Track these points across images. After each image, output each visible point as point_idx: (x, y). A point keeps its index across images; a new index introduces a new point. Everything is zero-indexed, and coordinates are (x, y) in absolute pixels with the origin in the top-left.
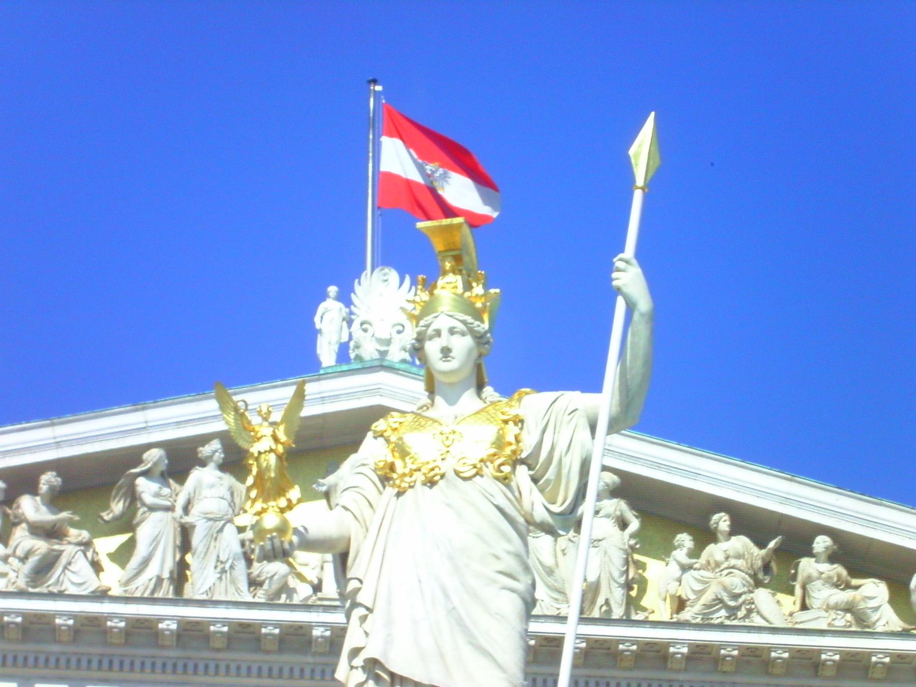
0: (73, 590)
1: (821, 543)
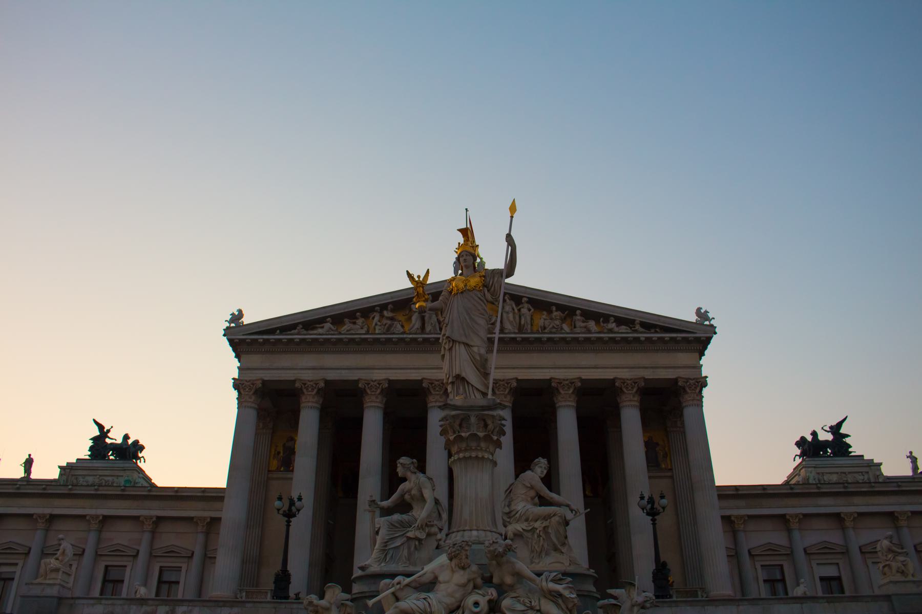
0: (397, 332)
1: (578, 312)
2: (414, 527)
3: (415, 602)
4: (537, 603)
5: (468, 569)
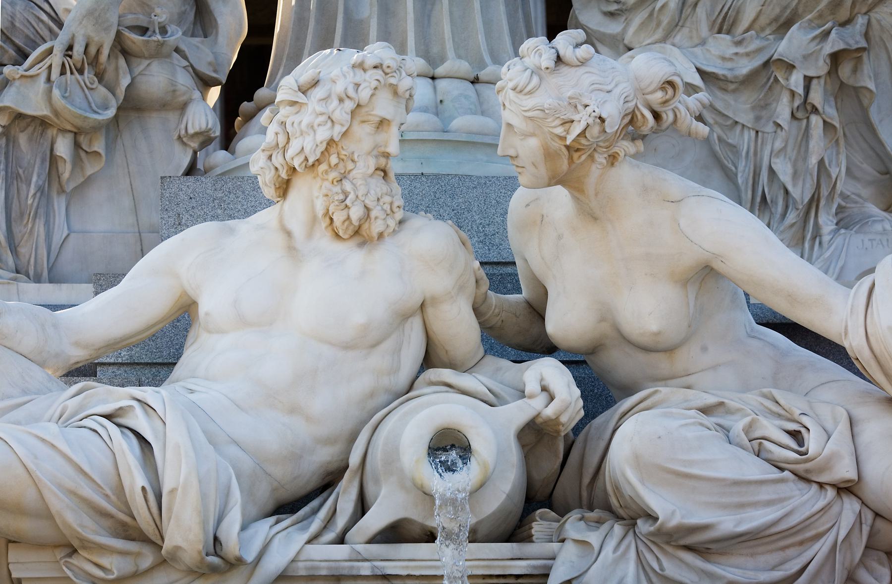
2: (50, 52)
3: (51, 431)
4: (839, 442)
5: (389, 243)
